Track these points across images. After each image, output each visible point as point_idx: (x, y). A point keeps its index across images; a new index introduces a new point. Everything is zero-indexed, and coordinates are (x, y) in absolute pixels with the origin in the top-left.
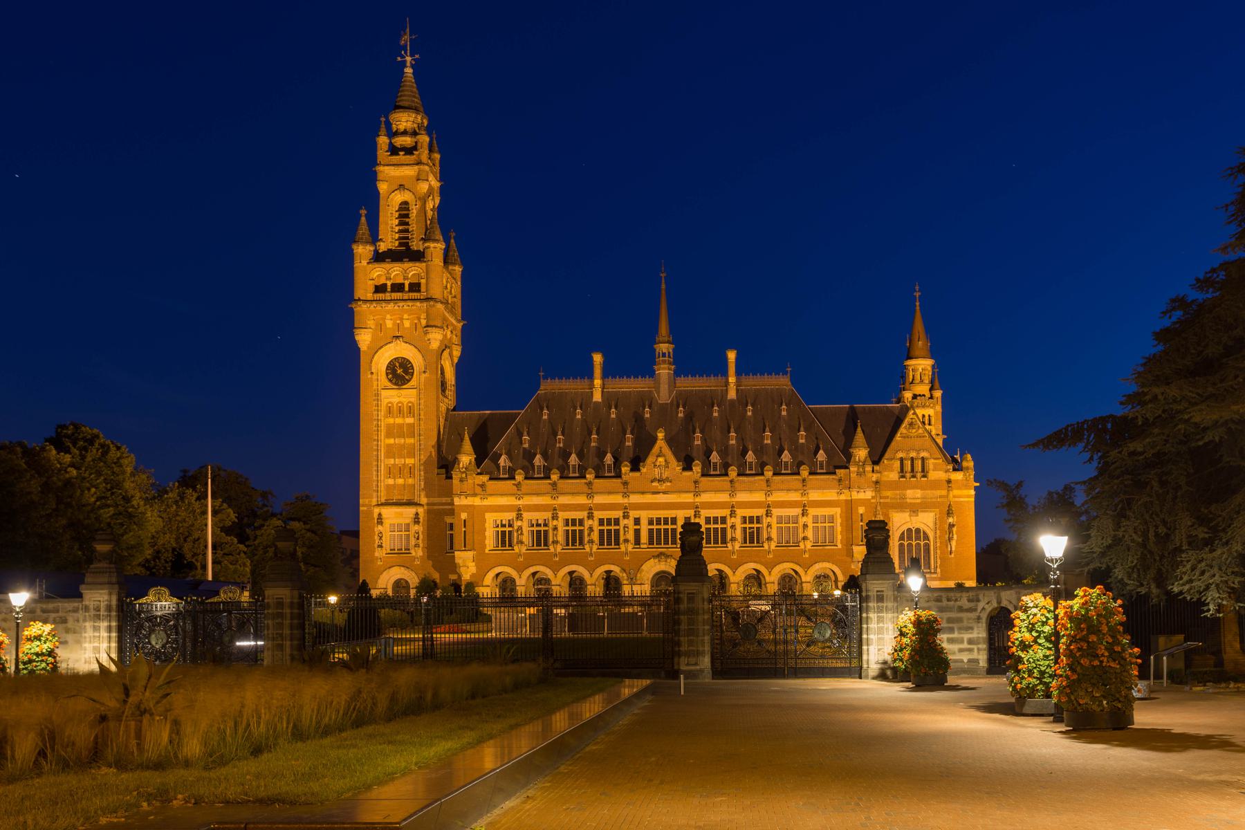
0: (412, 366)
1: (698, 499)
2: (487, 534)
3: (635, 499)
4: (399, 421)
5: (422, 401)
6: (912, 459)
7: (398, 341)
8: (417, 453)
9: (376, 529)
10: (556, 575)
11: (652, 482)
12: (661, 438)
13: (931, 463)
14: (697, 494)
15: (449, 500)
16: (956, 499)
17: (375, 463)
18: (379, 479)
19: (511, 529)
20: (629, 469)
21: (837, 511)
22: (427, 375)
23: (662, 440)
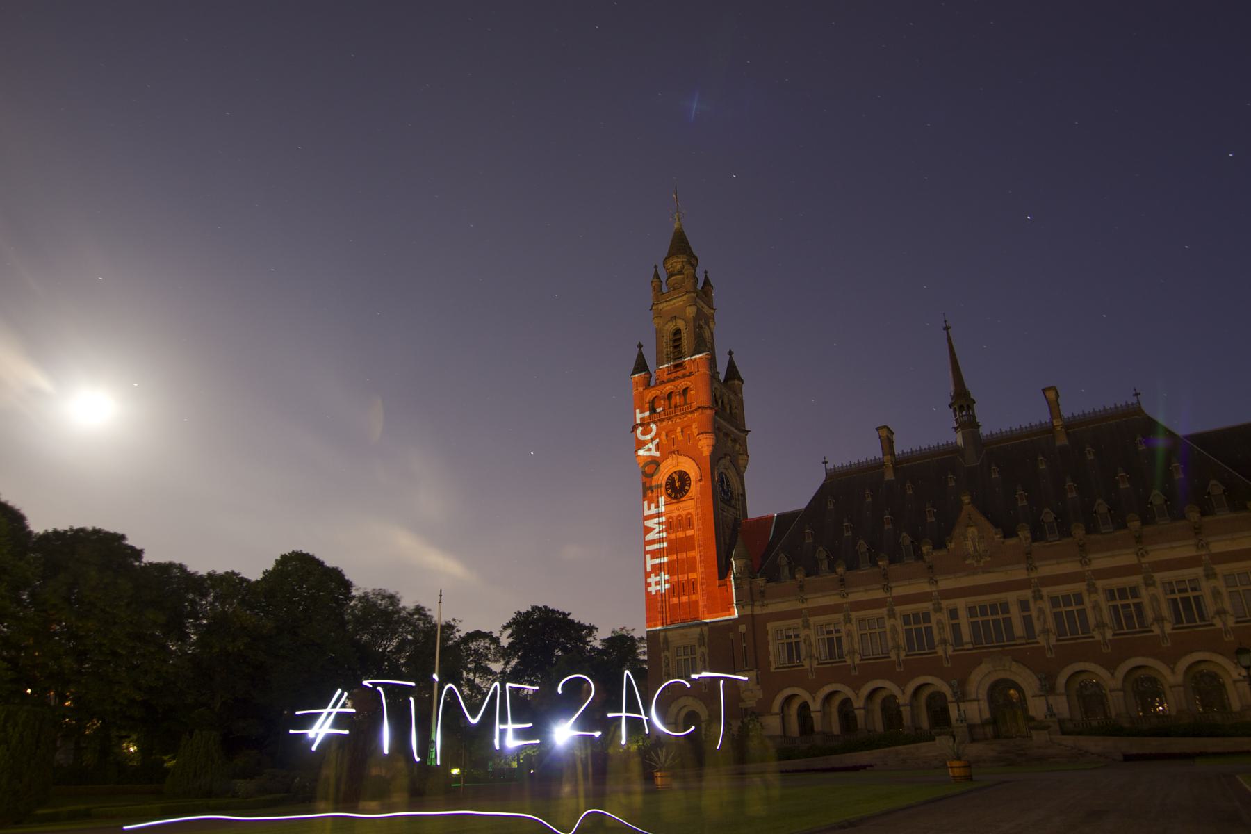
0: (689, 477)
1: (1033, 575)
2: (771, 648)
3: (946, 583)
4: (681, 534)
5: (699, 510)
7: (674, 455)
8: (698, 566)
9: (662, 655)
10: (857, 694)
12: (967, 501)
14: (1031, 568)
18: (664, 598)
19: (797, 640)
20: (931, 547)
22: (702, 483)
23: (969, 504)
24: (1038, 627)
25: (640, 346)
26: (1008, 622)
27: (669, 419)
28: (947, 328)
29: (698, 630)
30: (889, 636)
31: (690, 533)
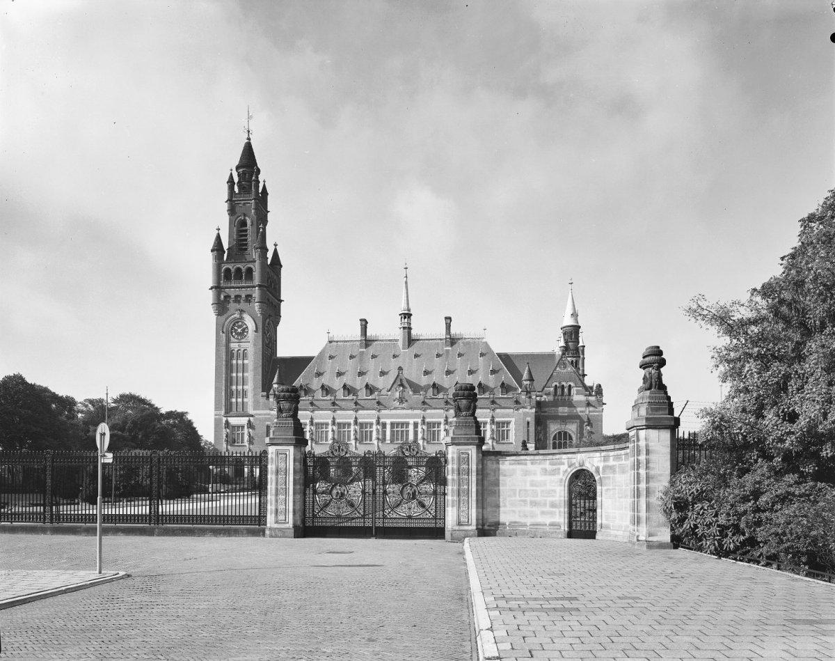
0: (247, 327)
6: (563, 387)
11: (394, 401)
13: (574, 391)
15: (268, 412)
16: (591, 414)
17: (224, 388)
21: (513, 420)
24: (420, 436)
25: (219, 229)
26: (407, 431)
27: (239, 288)
28: (406, 268)
29: (247, 418)
30: (352, 433)
31: (246, 362)
